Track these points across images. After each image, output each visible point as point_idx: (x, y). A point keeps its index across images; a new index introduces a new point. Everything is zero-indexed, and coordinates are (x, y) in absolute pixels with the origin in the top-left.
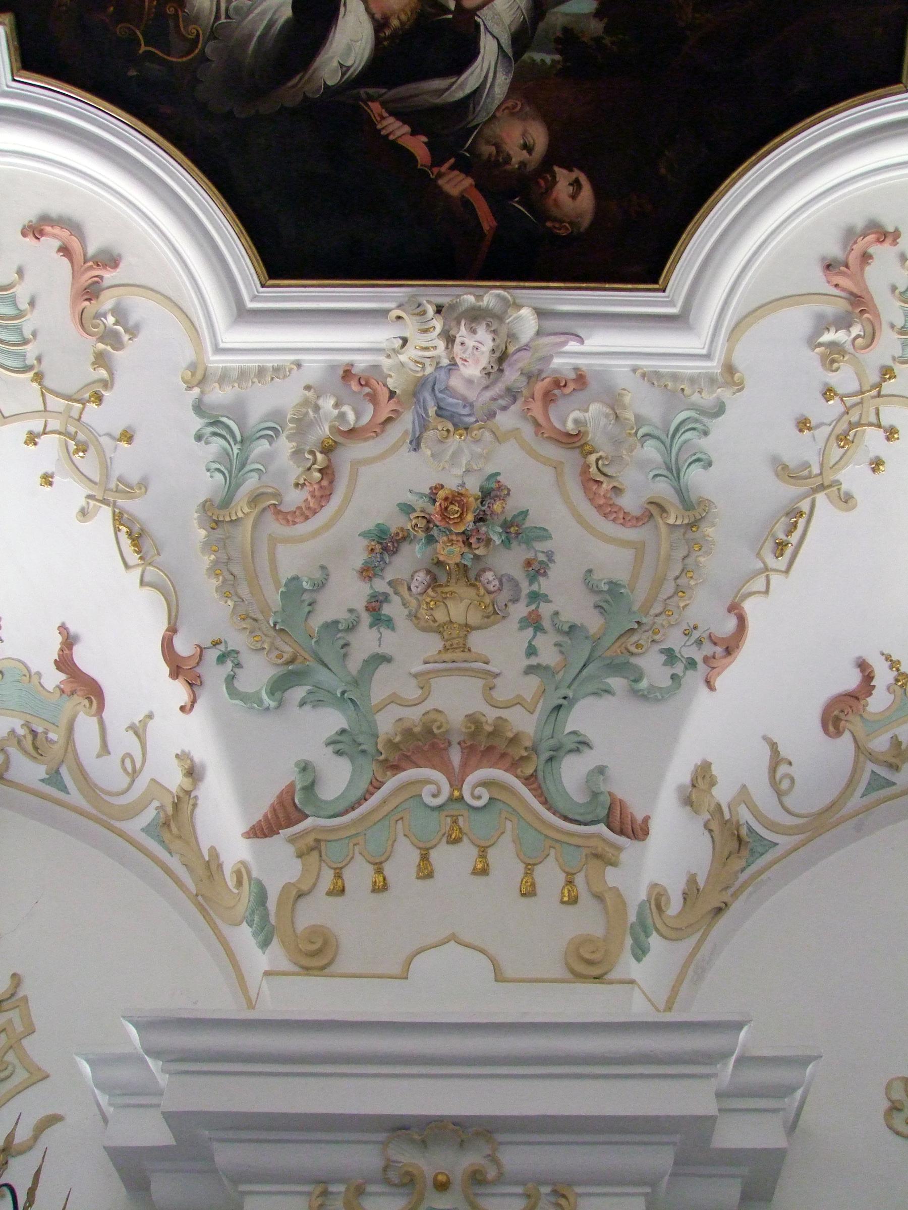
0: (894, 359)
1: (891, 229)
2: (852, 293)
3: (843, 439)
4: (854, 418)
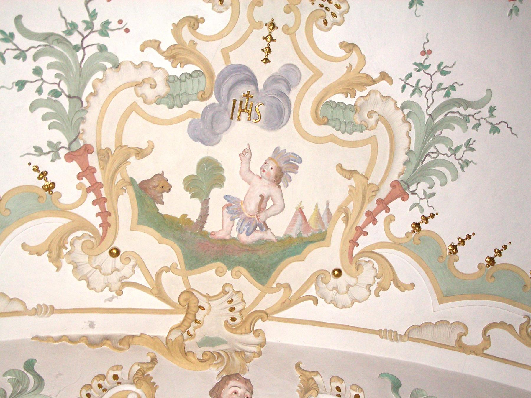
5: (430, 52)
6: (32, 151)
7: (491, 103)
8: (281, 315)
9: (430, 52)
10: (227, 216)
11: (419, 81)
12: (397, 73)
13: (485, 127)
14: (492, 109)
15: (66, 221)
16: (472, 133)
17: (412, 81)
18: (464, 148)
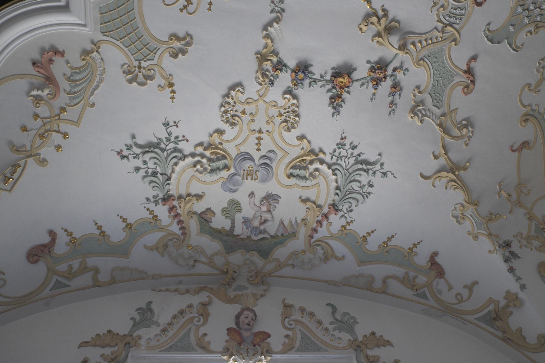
0: (66, 104)
1: (61, 50)
2: (45, 75)
3: (42, 136)
4: (48, 127)
5: (345, 138)
6: (146, 202)
7: (382, 161)
8: (277, 274)
9: (345, 138)
10: (245, 227)
11: (340, 153)
12: (328, 150)
13: (379, 174)
14: (382, 164)
15: (165, 234)
16: (371, 178)
17: (336, 154)
18: (367, 186)
